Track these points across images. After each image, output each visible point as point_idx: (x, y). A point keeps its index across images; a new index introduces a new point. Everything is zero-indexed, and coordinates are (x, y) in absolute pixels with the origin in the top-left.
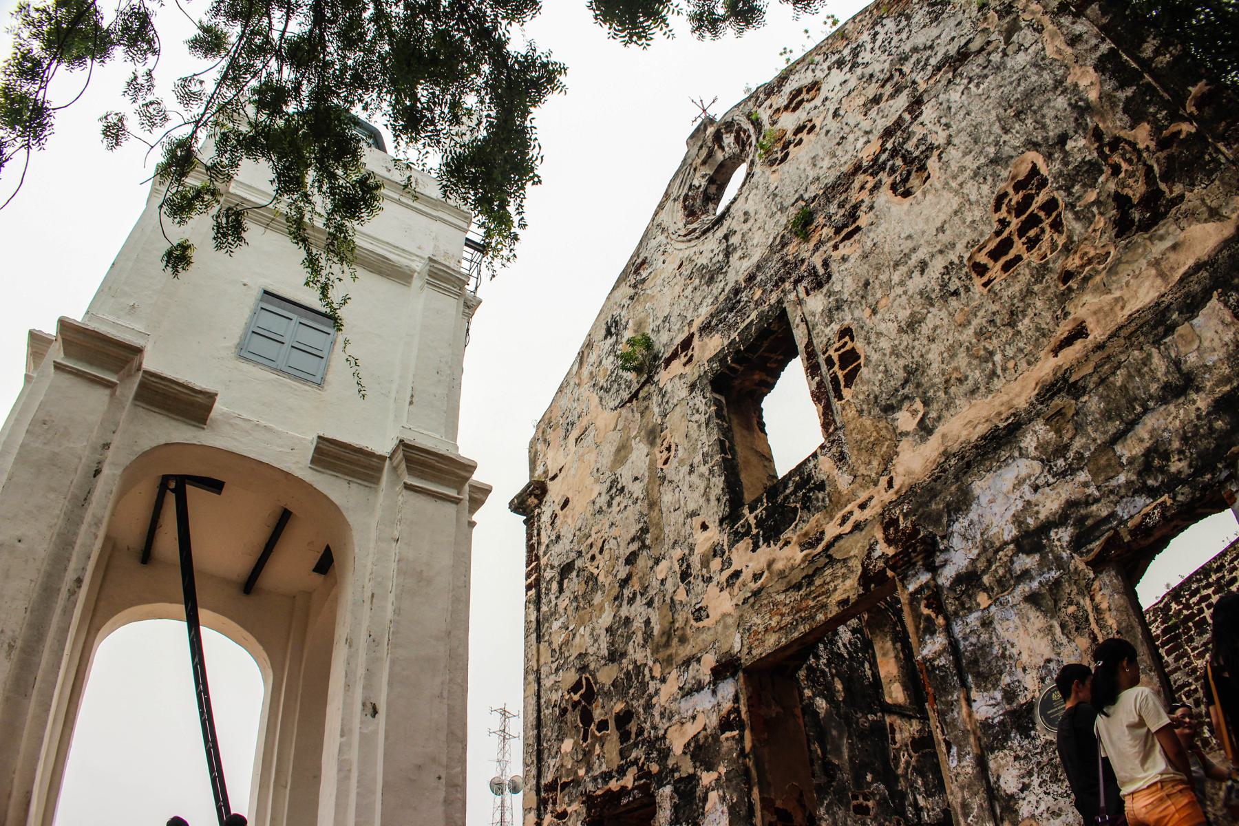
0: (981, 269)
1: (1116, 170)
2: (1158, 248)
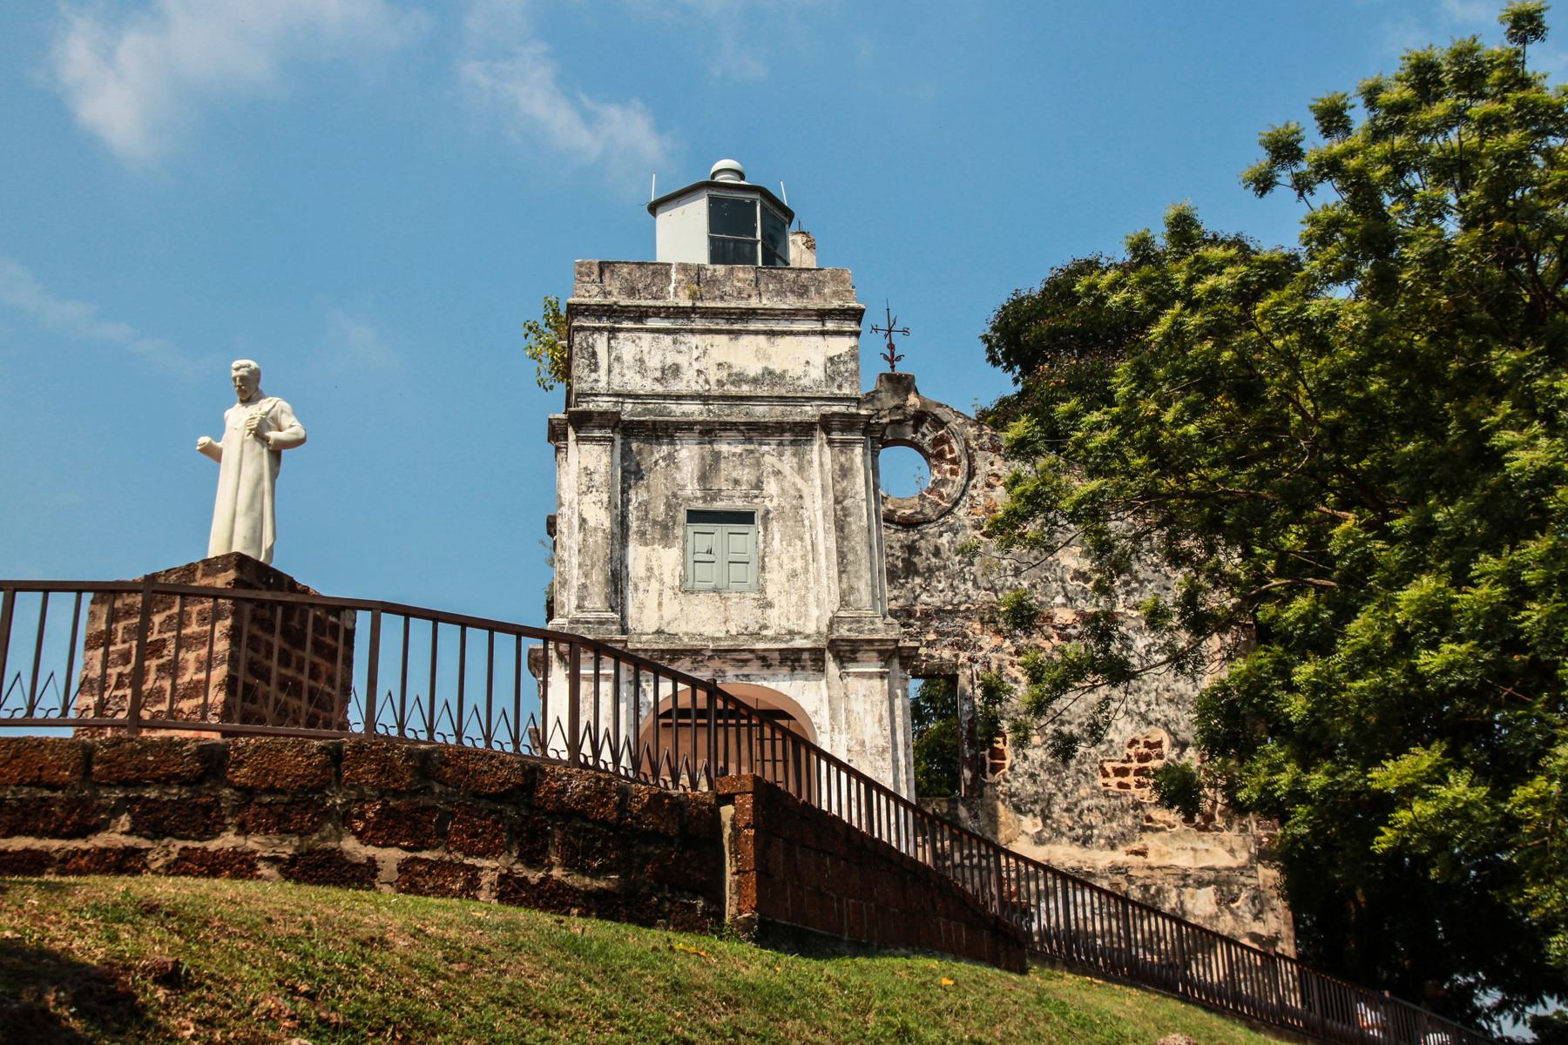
0: (1106, 775)
2: (1200, 845)
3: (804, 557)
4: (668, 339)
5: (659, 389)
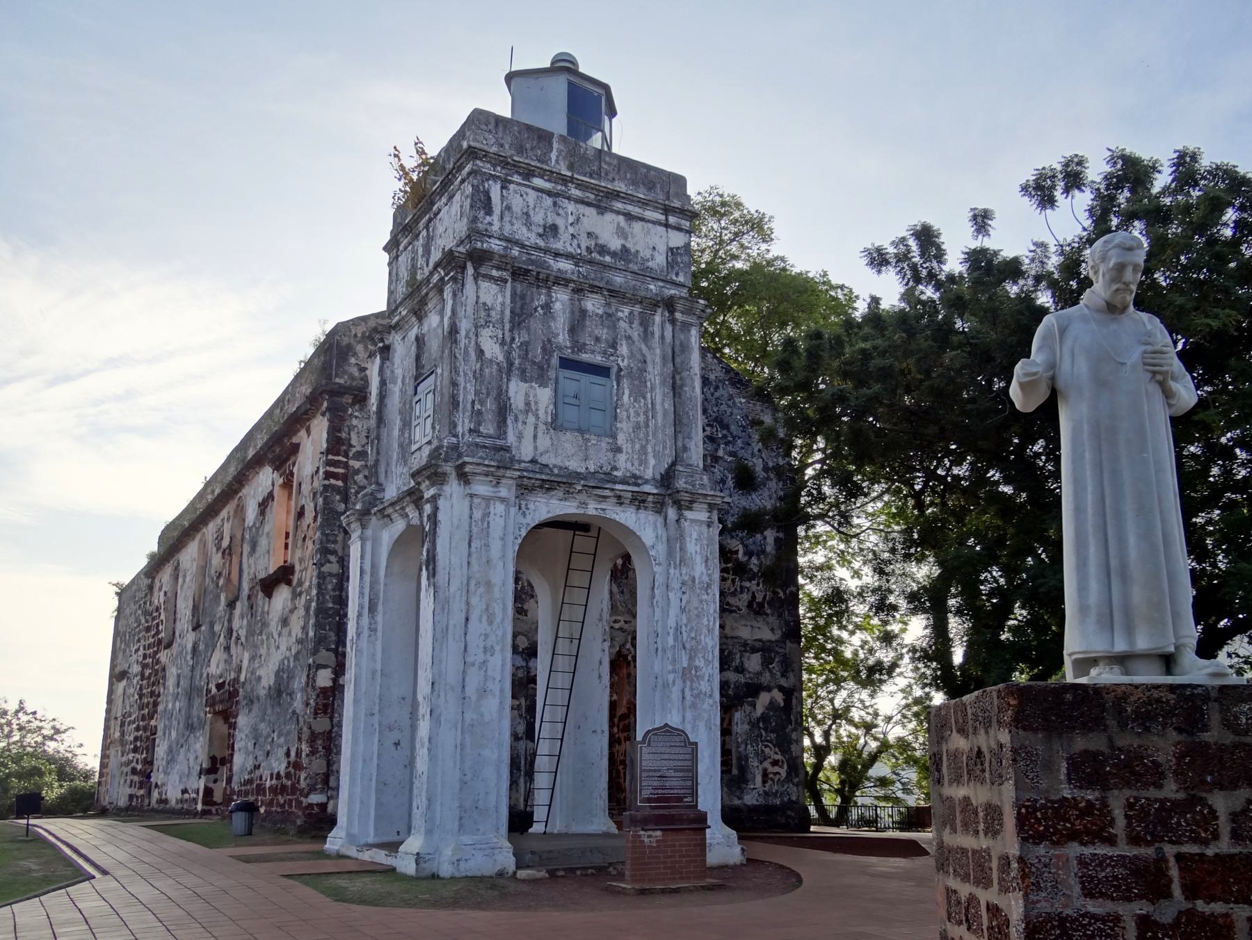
3: (646, 413)
4: (549, 201)
5: (541, 243)
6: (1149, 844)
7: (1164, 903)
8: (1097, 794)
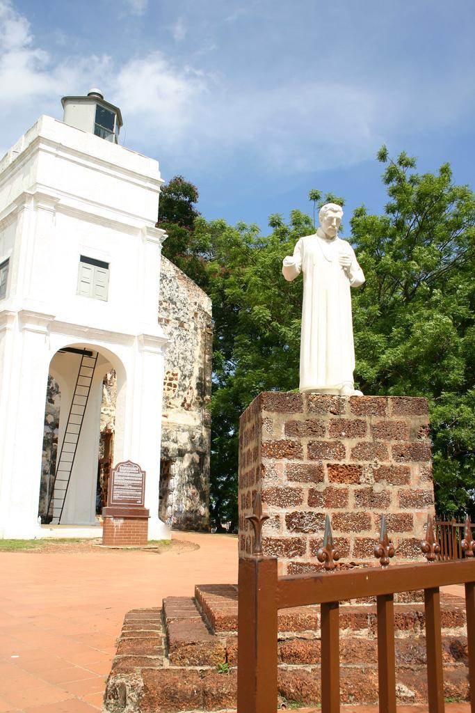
1: (188, 394)
6: (316, 459)
7: (321, 484)
8: (297, 439)
